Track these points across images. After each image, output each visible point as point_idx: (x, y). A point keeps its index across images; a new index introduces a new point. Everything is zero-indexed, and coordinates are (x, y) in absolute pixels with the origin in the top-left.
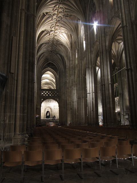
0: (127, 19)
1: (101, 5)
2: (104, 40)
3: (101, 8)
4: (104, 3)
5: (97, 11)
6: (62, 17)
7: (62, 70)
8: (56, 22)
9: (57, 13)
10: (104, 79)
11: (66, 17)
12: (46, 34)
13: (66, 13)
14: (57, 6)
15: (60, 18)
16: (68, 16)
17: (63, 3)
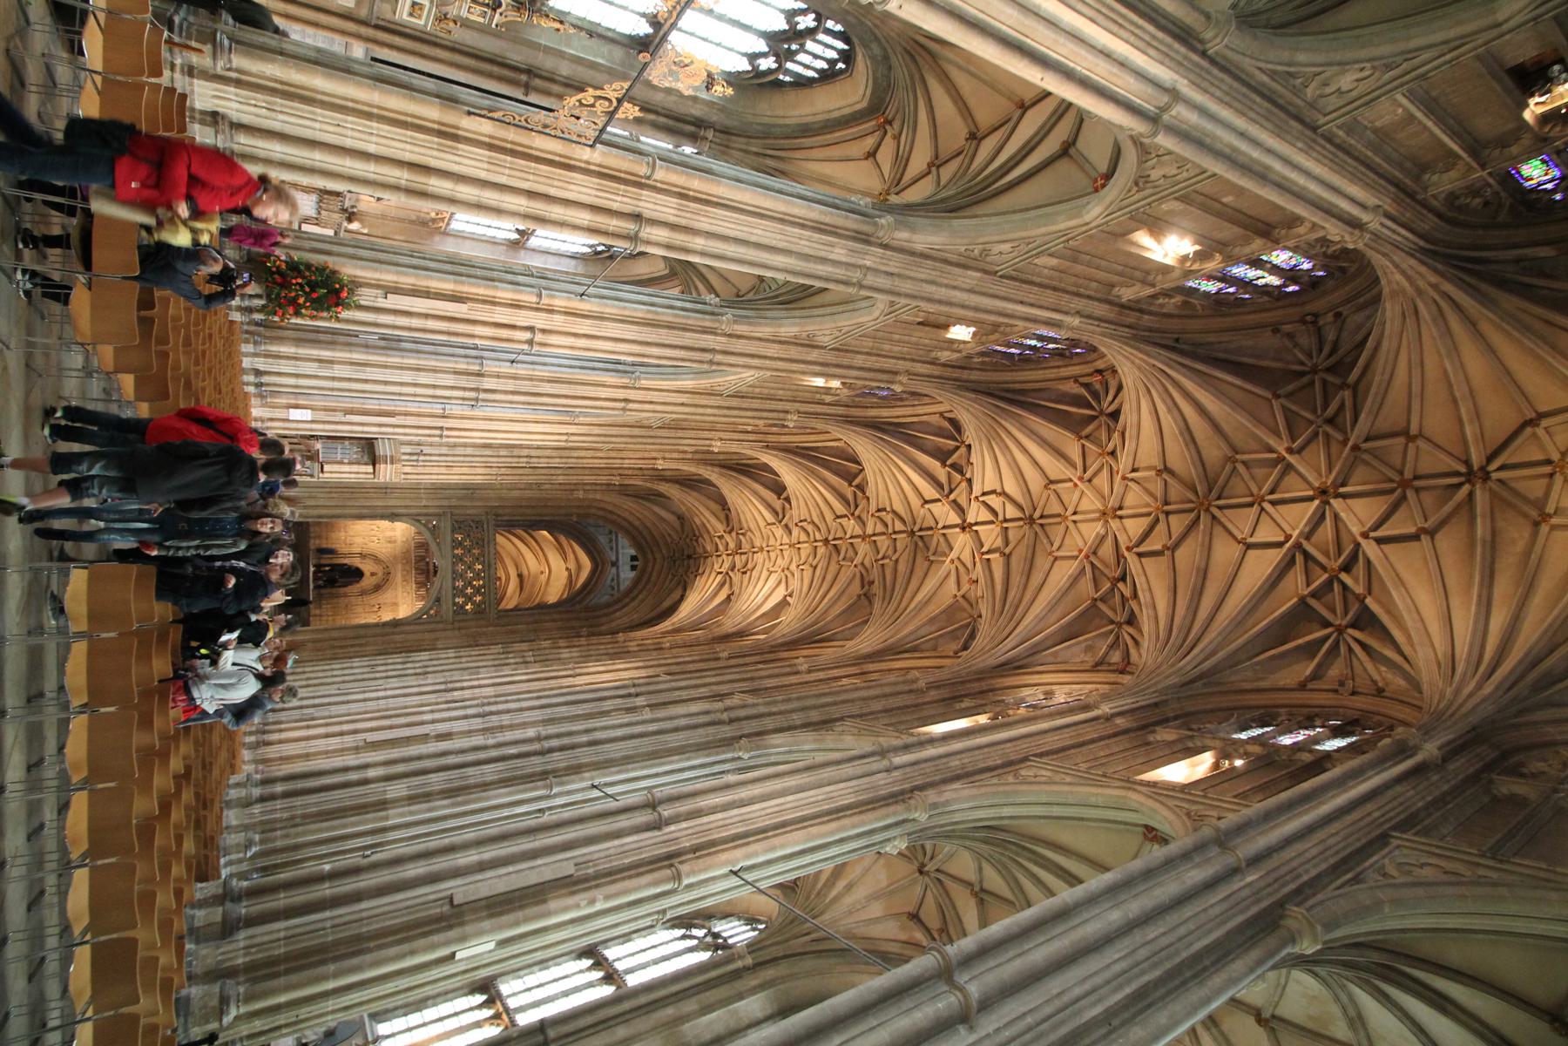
0: (922, 766)
1: (944, 693)
2: (791, 723)
3: (934, 695)
4: (958, 706)
5: (918, 679)
6: (857, 561)
7: (603, 620)
8: (830, 538)
9: (869, 531)
10: (573, 747)
11: (857, 582)
12: (769, 506)
13: (875, 574)
14: (899, 526)
15: (851, 553)
16: (867, 587)
17: (916, 544)
